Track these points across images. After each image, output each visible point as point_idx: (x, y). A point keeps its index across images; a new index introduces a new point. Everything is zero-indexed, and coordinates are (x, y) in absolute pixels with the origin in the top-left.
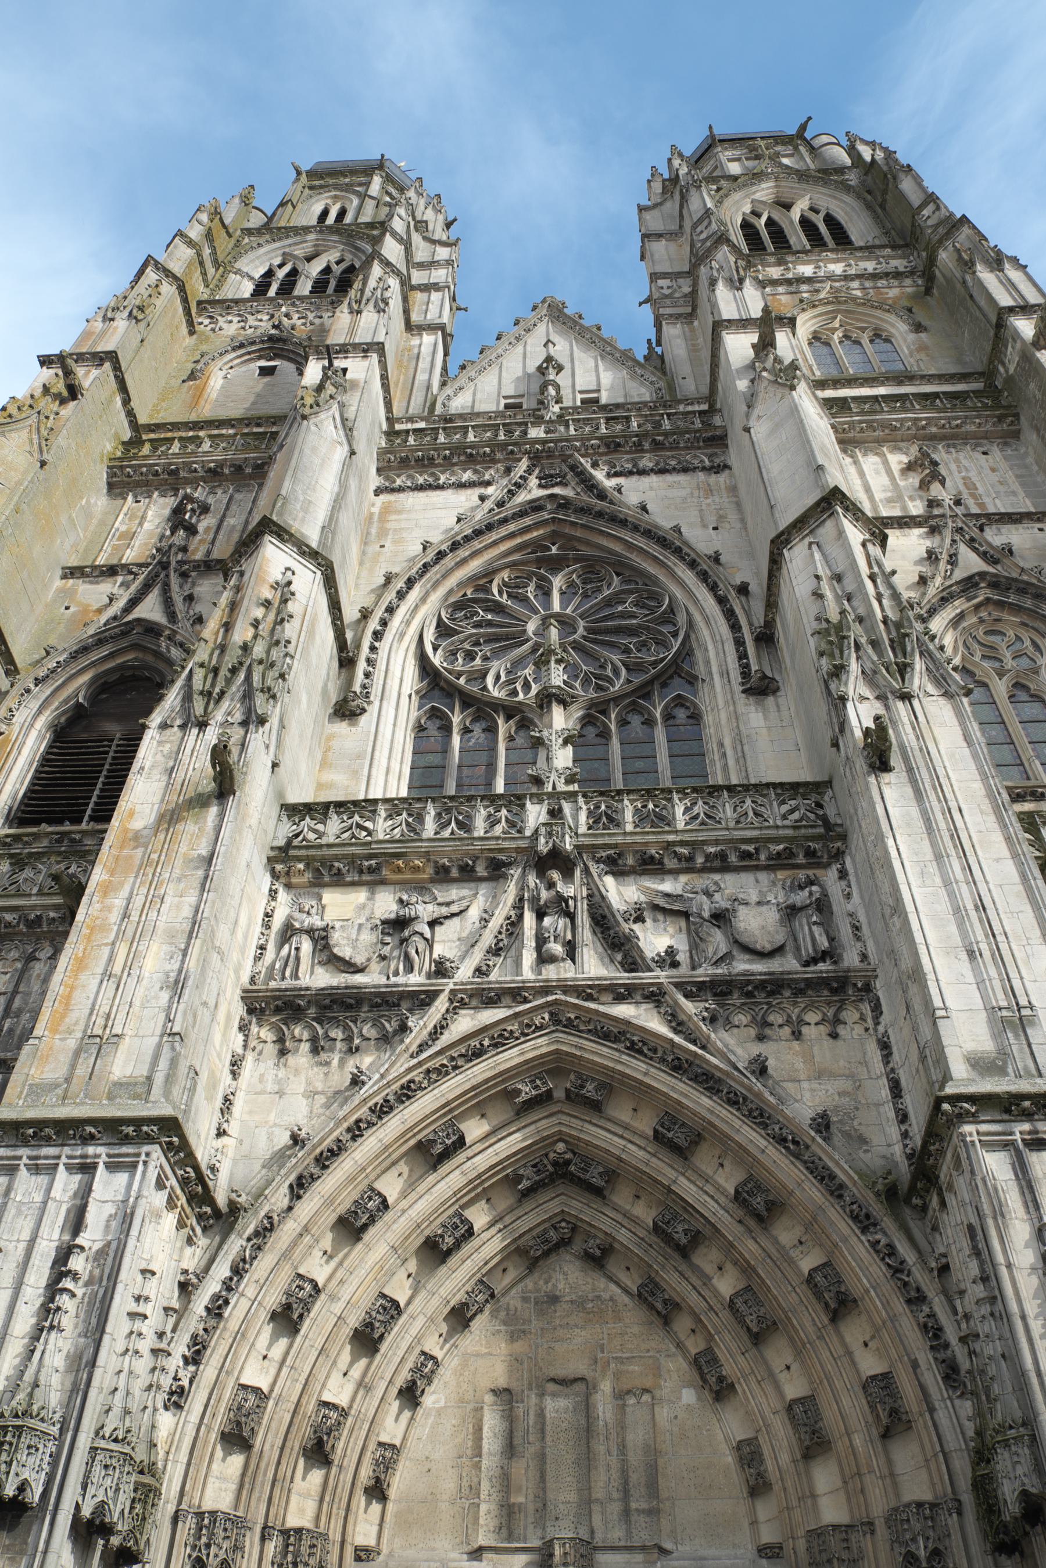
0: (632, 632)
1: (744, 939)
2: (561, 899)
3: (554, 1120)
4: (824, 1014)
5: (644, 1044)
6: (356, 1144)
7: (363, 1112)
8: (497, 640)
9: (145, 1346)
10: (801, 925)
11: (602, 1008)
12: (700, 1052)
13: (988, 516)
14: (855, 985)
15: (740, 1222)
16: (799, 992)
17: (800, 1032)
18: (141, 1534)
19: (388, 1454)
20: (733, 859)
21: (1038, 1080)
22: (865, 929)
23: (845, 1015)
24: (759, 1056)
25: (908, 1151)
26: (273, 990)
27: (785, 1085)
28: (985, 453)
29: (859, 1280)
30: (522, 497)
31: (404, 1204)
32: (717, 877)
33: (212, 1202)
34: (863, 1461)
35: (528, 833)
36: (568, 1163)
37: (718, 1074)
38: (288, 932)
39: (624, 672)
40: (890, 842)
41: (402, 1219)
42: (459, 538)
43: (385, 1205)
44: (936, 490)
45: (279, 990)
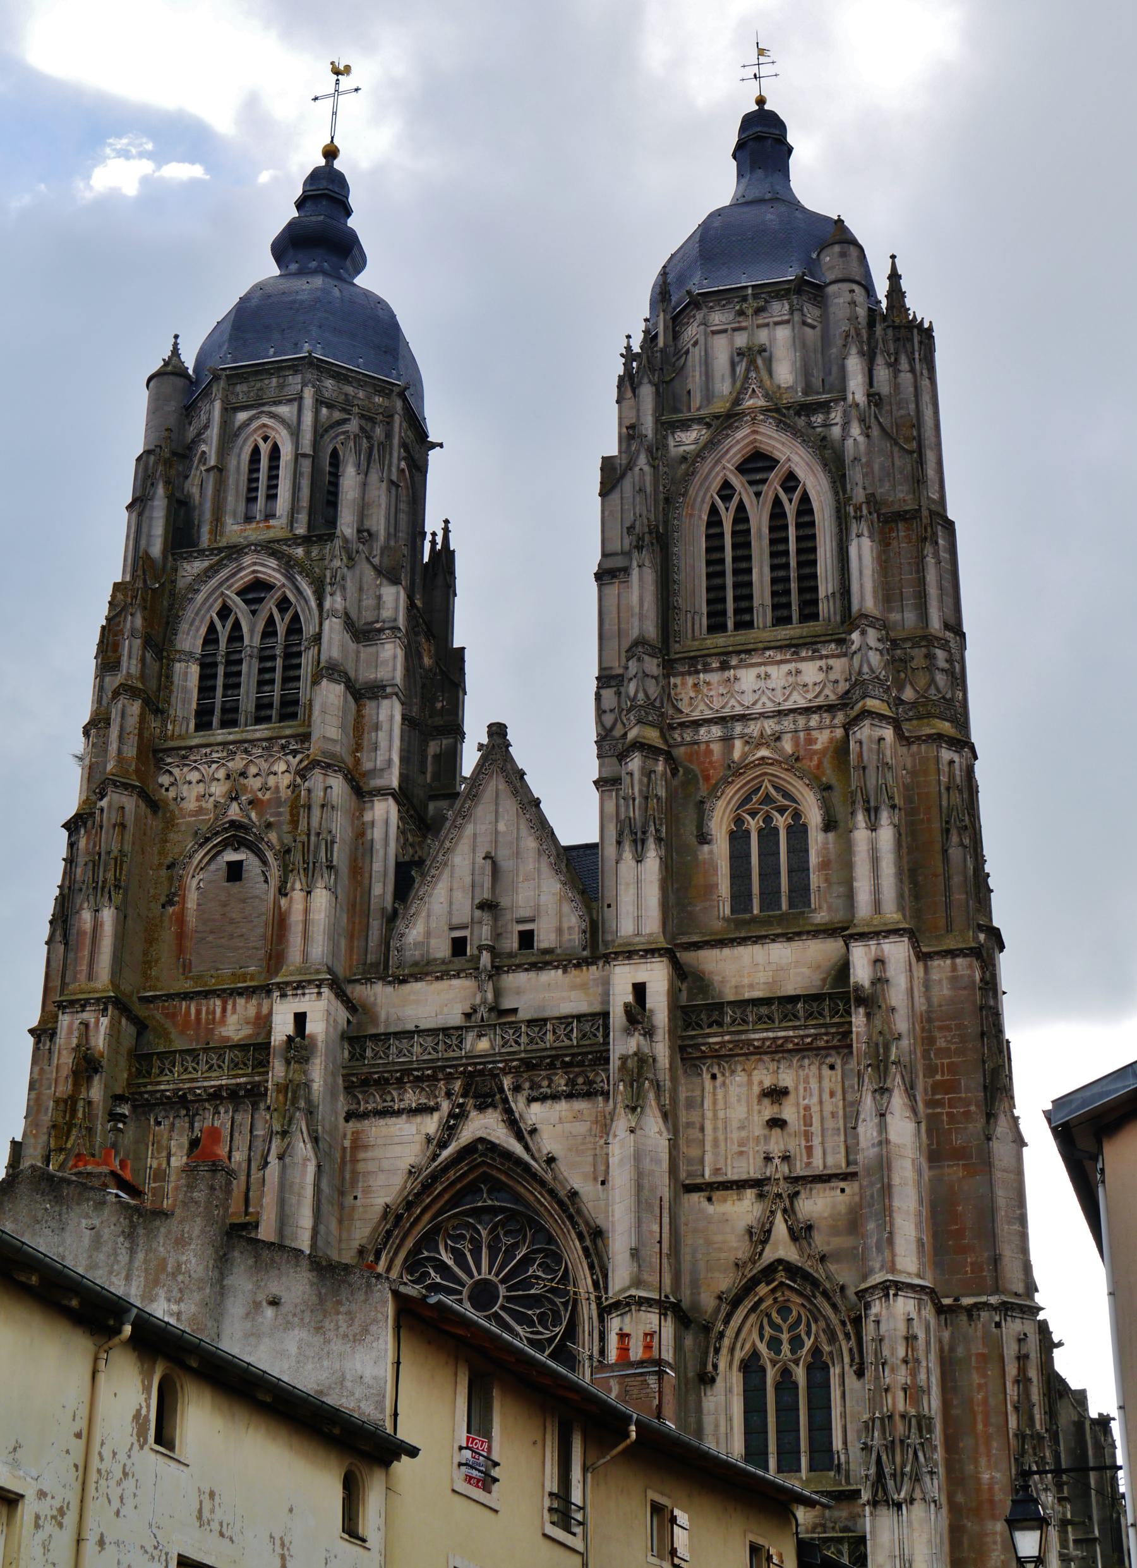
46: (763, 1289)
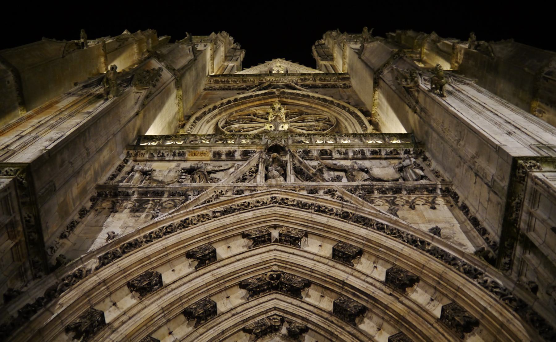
15: (391, 294)
22: (442, 172)
43: (160, 282)
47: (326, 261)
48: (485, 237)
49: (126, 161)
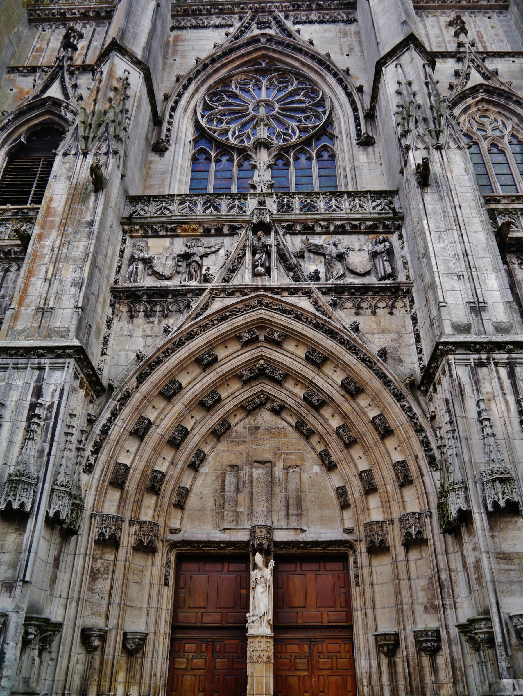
0: (302, 110)
1: (352, 267)
2: (265, 246)
3: (259, 350)
4: (387, 304)
5: (302, 315)
6: (167, 359)
7: (170, 345)
8: (234, 113)
9: (73, 447)
10: (379, 261)
11: (282, 299)
12: (328, 320)
13: (487, 53)
14: (403, 290)
15: (343, 396)
16: (376, 293)
17: (375, 312)
18: (76, 523)
19: (184, 491)
20: (348, 228)
21: (484, 336)
22: (409, 263)
23: (397, 304)
24: (356, 322)
25: (421, 366)
26: (125, 288)
27: (367, 335)
28: (489, 18)
29: (395, 421)
30: (248, 35)
31: (190, 386)
32: (339, 237)
33: (101, 385)
34: (390, 496)
35: (248, 213)
36: (266, 368)
37: (336, 330)
38: (133, 260)
39: (298, 132)
40: (425, 222)
41: (189, 393)
42: (215, 56)
43: (180, 387)
44: (462, 37)
45: (129, 287)
46: (470, 101)
47: (300, 360)
48: (420, 356)
49: (124, 241)
